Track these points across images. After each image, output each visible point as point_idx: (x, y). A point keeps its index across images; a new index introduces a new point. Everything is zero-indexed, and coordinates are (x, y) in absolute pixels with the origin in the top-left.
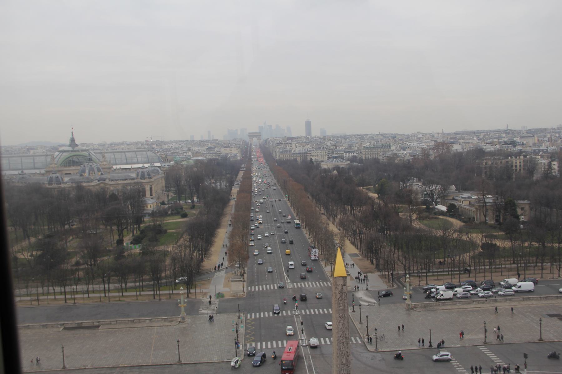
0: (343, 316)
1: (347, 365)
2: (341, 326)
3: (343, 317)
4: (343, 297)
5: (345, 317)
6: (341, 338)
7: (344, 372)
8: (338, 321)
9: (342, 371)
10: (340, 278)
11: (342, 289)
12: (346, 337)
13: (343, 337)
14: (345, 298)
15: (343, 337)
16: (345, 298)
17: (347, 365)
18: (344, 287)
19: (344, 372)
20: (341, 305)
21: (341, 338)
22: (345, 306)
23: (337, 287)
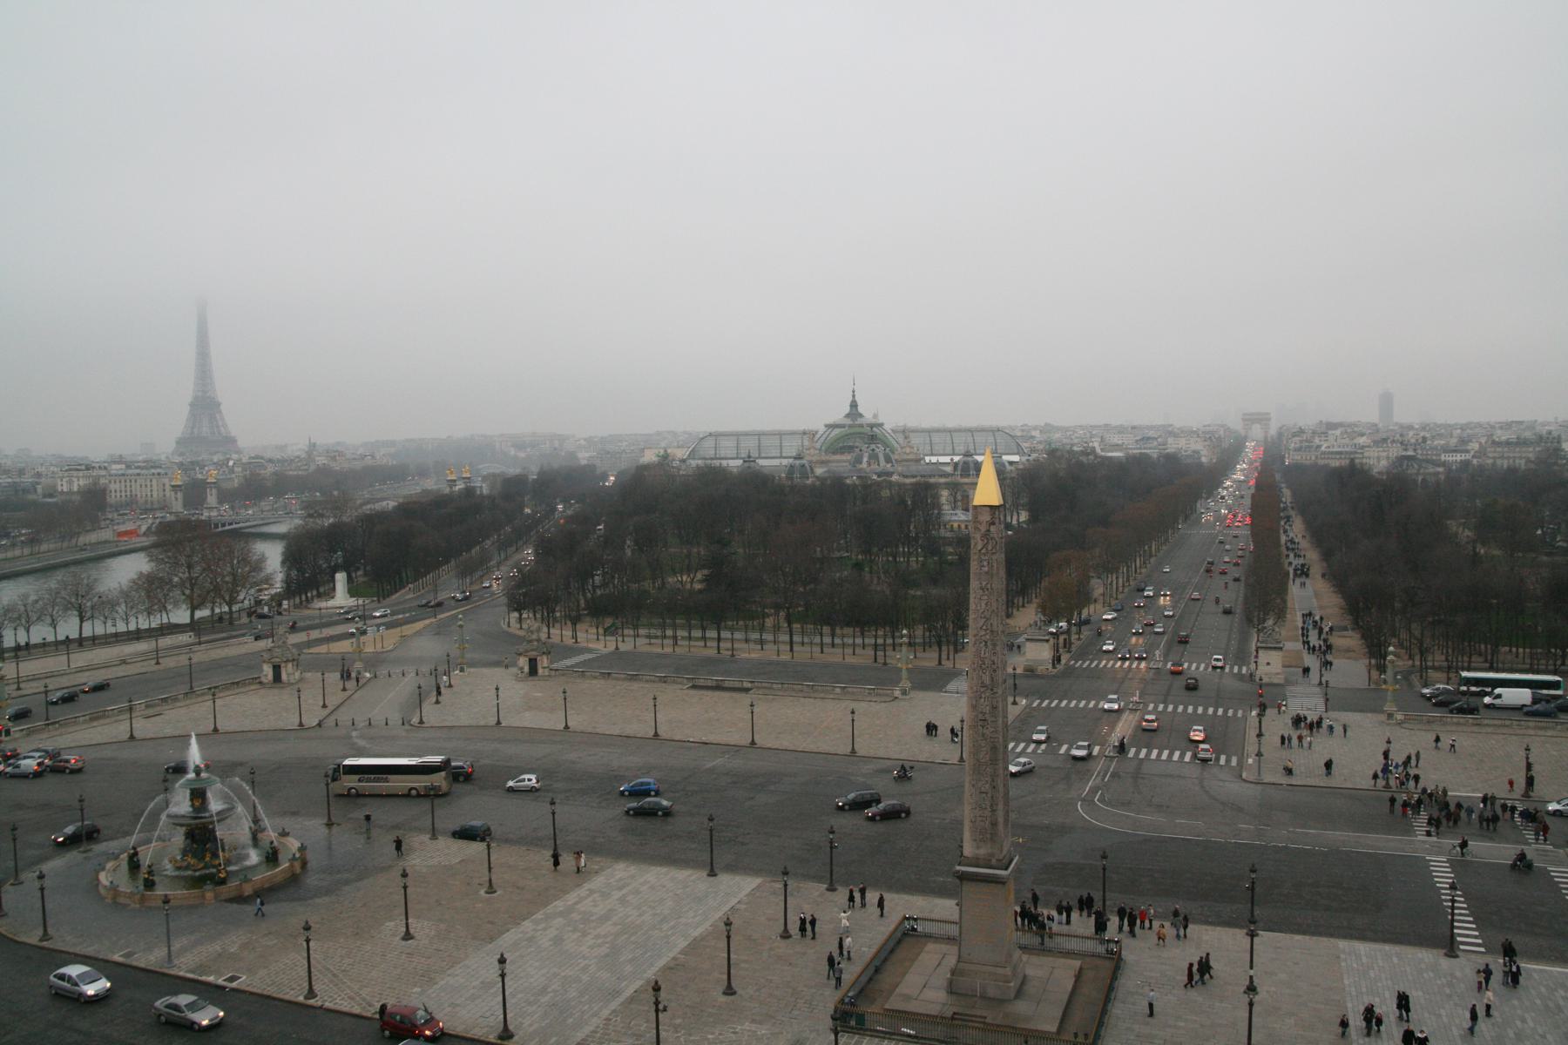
1: (992, 690)
2: (983, 605)
4: (990, 548)
7: (986, 703)
9: (983, 700)
10: (984, 508)
11: (989, 531)
12: (992, 631)
13: (986, 630)
14: (994, 551)
15: (986, 630)
16: (994, 551)
17: (992, 690)
18: (993, 529)
19: (986, 703)
20: (985, 563)
22: (992, 566)
23: (979, 526)
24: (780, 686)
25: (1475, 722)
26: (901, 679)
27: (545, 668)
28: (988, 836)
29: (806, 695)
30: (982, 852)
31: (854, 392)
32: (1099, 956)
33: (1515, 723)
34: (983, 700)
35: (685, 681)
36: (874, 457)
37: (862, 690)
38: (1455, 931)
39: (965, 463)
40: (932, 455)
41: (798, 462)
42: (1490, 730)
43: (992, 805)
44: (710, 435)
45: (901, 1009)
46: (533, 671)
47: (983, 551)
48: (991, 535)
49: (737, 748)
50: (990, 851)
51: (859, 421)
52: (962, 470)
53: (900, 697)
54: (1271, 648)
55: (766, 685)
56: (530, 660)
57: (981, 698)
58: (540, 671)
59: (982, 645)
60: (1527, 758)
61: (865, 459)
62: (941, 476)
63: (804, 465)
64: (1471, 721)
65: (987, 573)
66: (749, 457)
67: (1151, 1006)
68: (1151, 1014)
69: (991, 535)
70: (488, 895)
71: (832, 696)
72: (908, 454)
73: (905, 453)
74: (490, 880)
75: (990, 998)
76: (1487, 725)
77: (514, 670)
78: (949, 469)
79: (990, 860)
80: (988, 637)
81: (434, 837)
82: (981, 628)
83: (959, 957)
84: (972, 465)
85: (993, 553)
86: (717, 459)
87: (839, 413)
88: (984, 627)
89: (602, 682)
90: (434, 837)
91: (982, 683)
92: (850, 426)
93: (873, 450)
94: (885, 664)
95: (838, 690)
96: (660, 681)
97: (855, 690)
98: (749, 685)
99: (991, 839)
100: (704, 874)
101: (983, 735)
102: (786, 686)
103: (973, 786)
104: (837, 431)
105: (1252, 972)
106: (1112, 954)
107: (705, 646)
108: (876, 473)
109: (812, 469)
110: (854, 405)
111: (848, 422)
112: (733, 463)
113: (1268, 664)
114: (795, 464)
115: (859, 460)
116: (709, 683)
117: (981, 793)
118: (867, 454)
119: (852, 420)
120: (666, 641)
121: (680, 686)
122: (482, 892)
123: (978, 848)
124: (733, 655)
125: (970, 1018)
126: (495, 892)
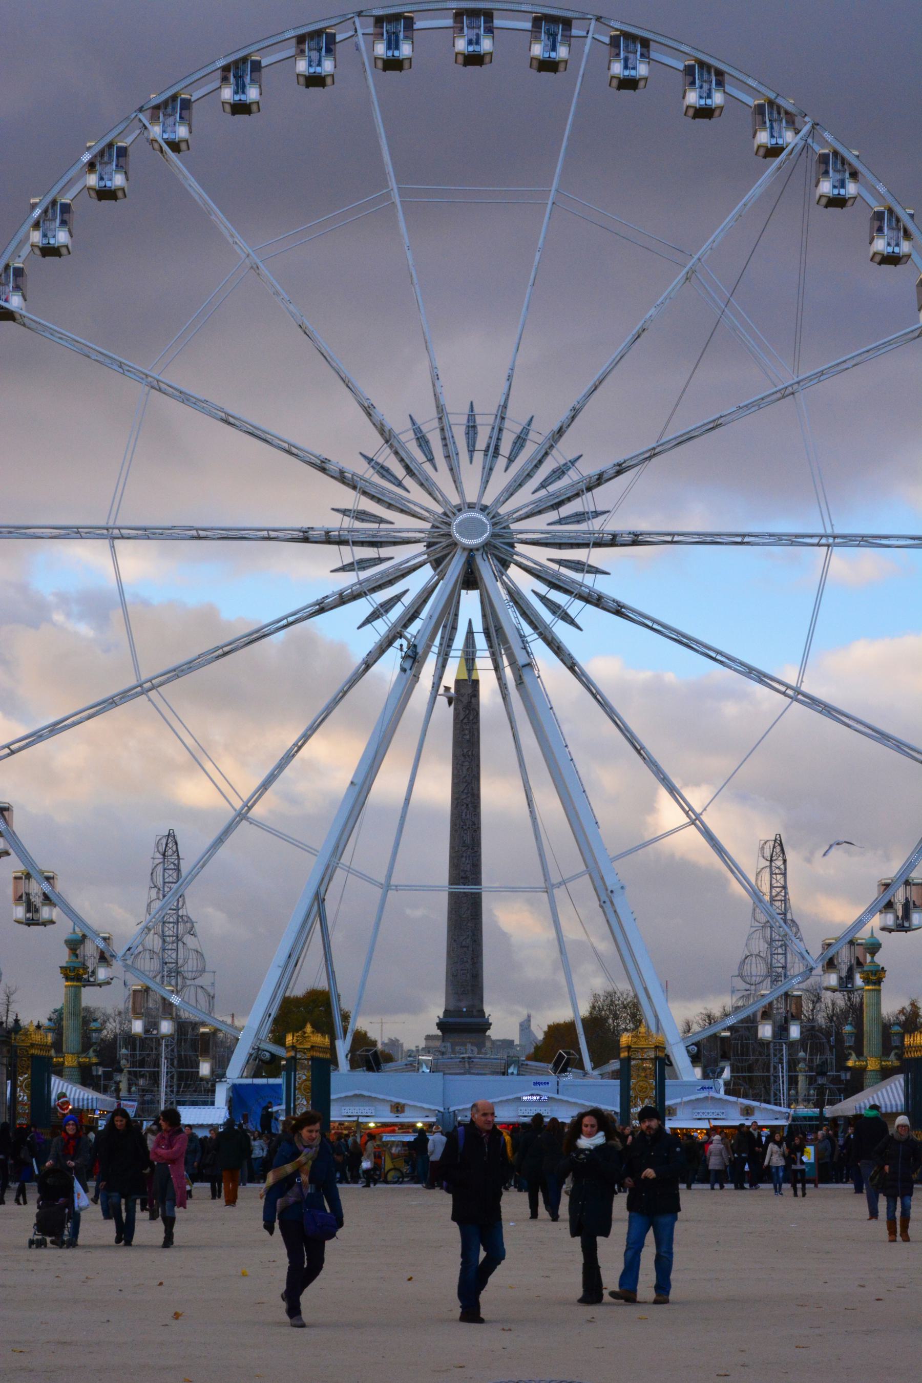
0: (470, 753)
1: (473, 849)
2: (465, 772)
3: (469, 756)
4: (471, 718)
5: (472, 755)
9: (464, 859)
11: (470, 702)
13: (467, 793)
14: (475, 720)
15: (467, 793)
17: (473, 849)
20: (467, 732)
43: (473, 959)
47: (464, 721)
57: (462, 856)
59: (463, 808)
65: (468, 741)
79: (472, 1011)
82: (462, 792)
88: (466, 791)
103: (455, 941)
117: (462, 947)
123: (460, 1000)
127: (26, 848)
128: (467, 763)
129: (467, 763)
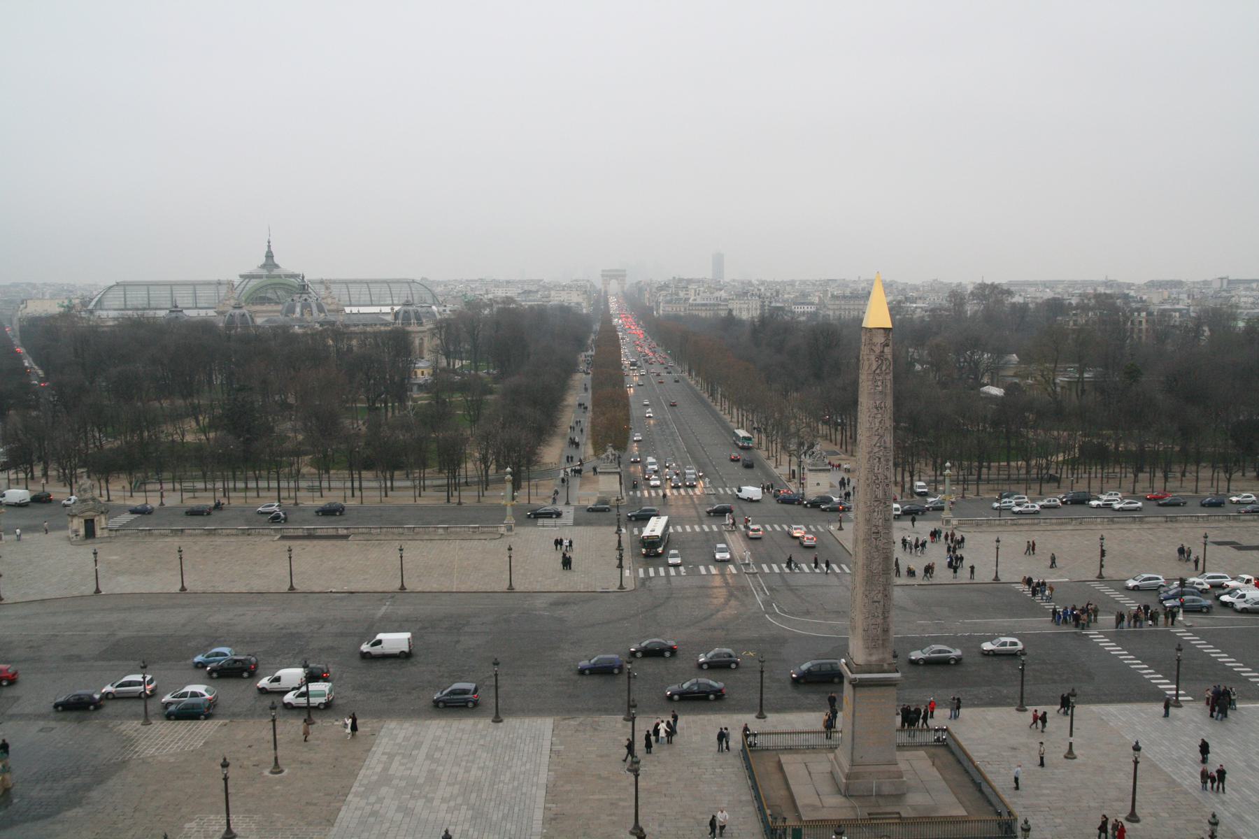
1: (885, 503)
2: (877, 425)
3: (881, 408)
4: (884, 368)
6: (876, 450)
8: (872, 415)
9: (876, 514)
11: (883, 352)
12: (885, 448)
13: (880, 447)
14: (888, 371)
16: (888, 371)
18: (887, 350)
20: (879, 383)
21: (876, 450)
22: (886, 386)
23: (873, 347)
24: (379, 530)
25: (1013, 522)
26: (506, 516)
27: (103, 529)
28: (880, 642)
29: (410, 538)
30: (874, 658)
31: (269, 242)
32: (926, 745)
33: (1042, 521)
34: (876, 514)
35: (272, 532)
36: (306, 305)
37: (466, 529)
38: (1175, 686)
39: (406, 312)
40: (350, 305)
41: (237, 312)
42: (1026, 528)
43: (883, 613)
44: (118, 284)
45: (820, 818)
46: (90, 532)
48: (885, 356)
49: (383, 595)
50: (881, 656)
51: (276, 272)
52: (403, 320)
53: (506, 533)
54: (820, 470)
55: (364, 530)
56: (86, 521)
57: (874, 511)
58: (98, 533)
60: (1102, 546)
61: (298, 310)
62: (382, 325)
63: (244, 315)
64: (1009, 522)
66: (176, 307)
67: (1016, 780)
68: (1017, 788)
69: (885, 356)
70: (271, 775)
71: (437, 538)
72: (330, 305)
73: (327, 304)
74: (276, 759)
75: (884, 796)
76: (1022, 524)
77: (63, 533)
78: (390, 318)
79: (882, 665)
80: (881, 453)
81: (147, 722)
83: (852, 760)
84: (412, 314)
85: (886, 374)
86: (150, 309)
87: (254, 263)
89: (177, 539)
90: (147, 722)
91: (876, 497)
92: (267, 277)
93: (306, 300)
94: (460, 503)
95: (441, 531)
96: (243, 533)
97: (458, 530)
98: (345, 532)
99: (883, 644)
100: (489, 721)
101: (876, 546)
102: (385, 530)
104: (254, 282)
105: (1071, 740)
106: (939, 741)
107: (258, 496)
108: (318, 323)
109: (252, 319)
110: (269, 256)
111: (264, 272)
112: (161, 313)
113: (818, 484)
114: (235, 313)
115: (291, 310)
116: (300, 533)
118: (299, 304)
119: (268, 271)
120: (249, 494)
121: (271, 538)
122: (266, 773)
123: (871, 655)
124: (296, 504)
125: (883, 816)
126: (281, 772)
127: (963, 744)
128: (879, 416)
129: (879, 416)
